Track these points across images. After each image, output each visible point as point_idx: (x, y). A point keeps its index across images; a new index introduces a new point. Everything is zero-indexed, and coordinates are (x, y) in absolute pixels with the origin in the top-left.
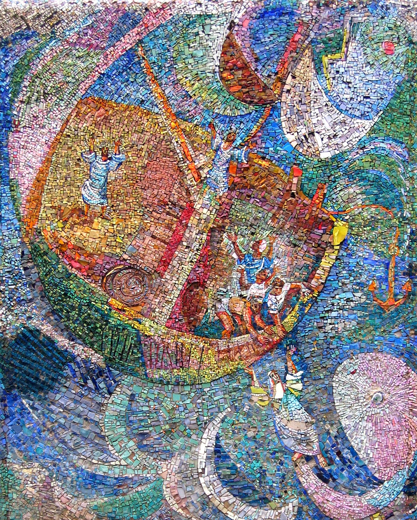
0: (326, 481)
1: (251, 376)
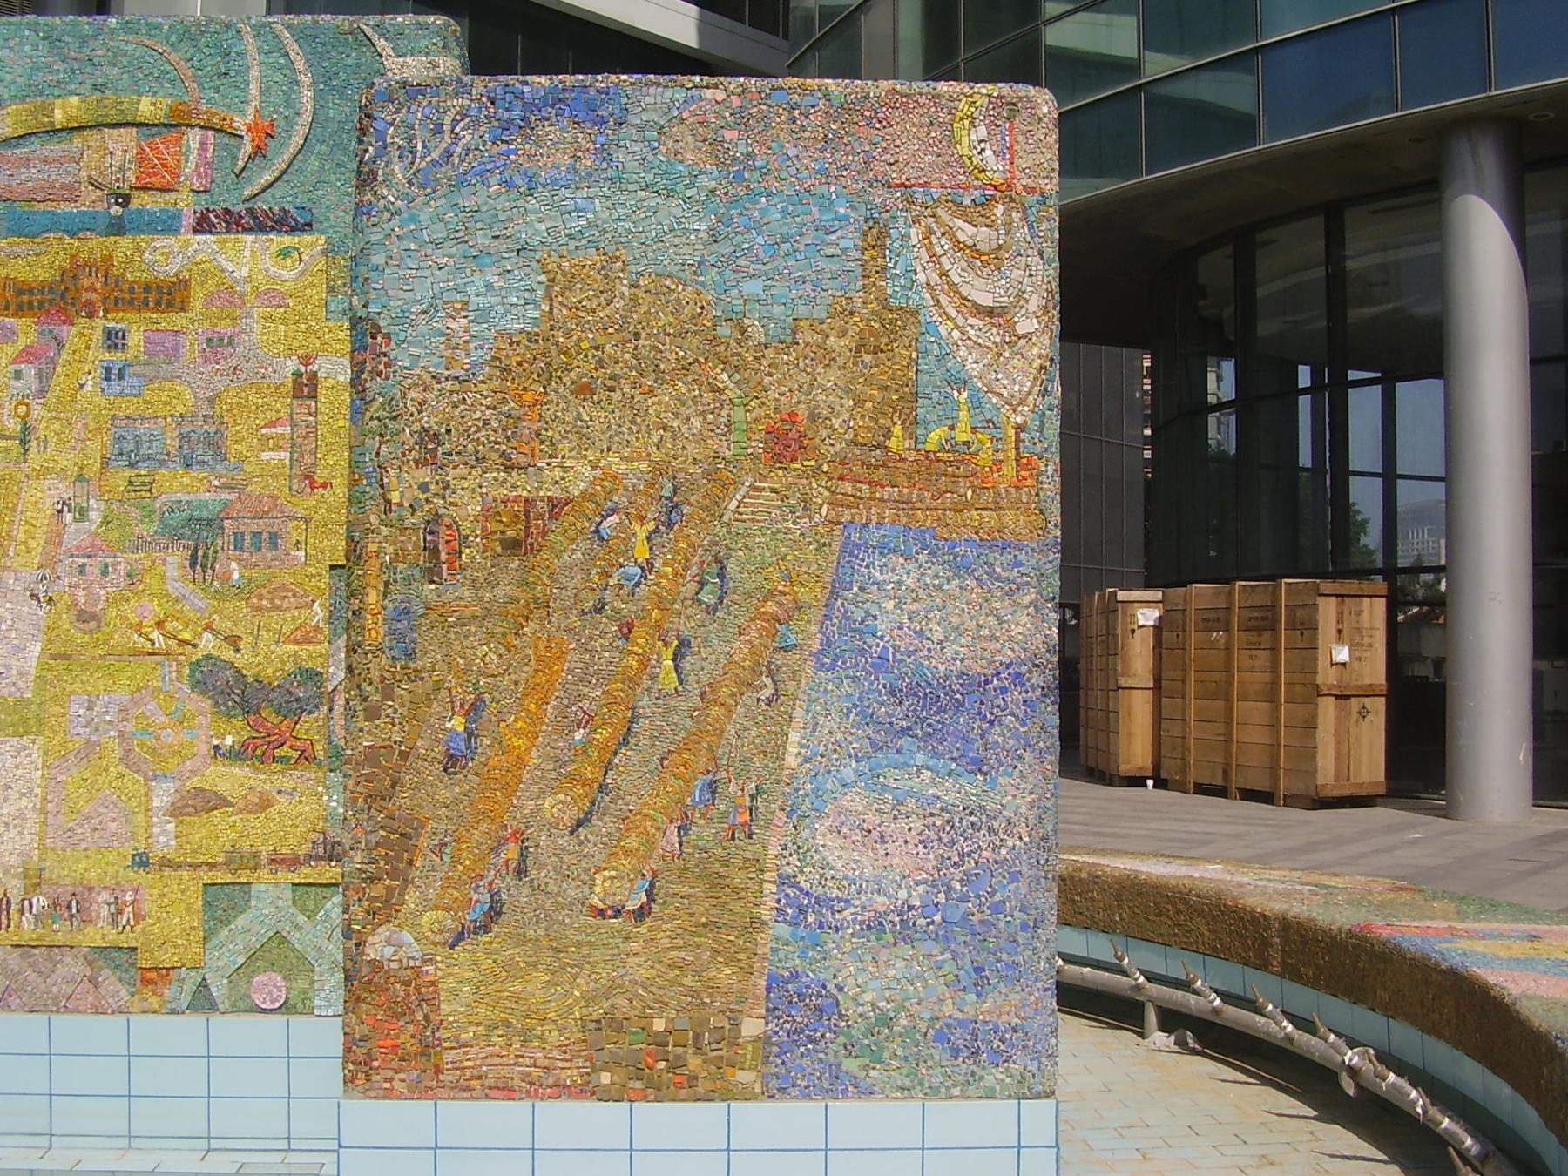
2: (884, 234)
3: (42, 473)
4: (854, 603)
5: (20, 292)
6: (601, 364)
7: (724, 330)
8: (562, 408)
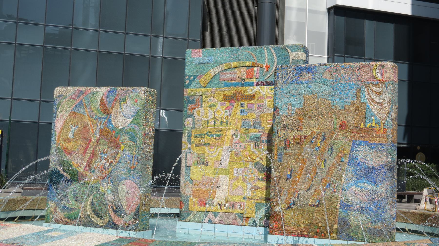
1: (100, 183)
2: (360, 90)
3: (229, 129)
5: (226, 97)
7: (333, 107)
8: (306, 120)
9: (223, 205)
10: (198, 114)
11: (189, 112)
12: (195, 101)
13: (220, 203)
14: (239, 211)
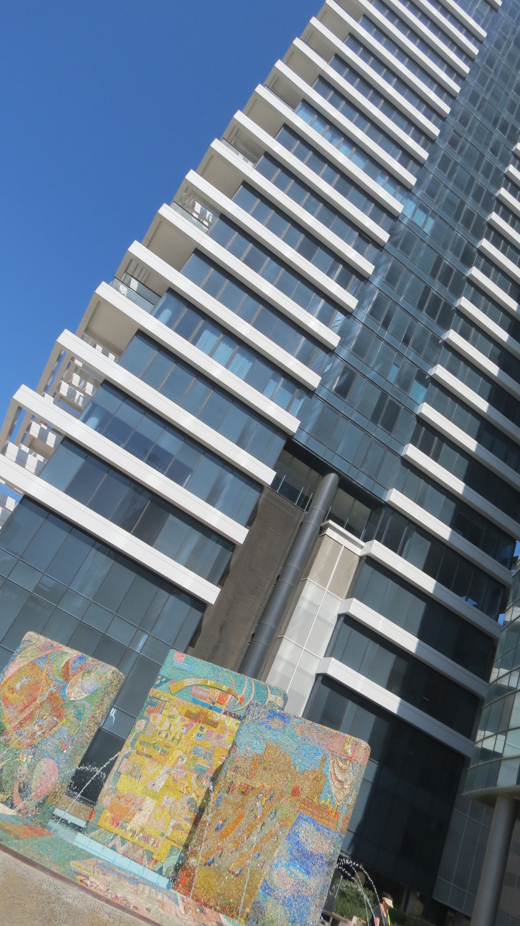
0: (19, 792)
2: (326, 759)
3: (179, 749)
4: (297, 828)
5: (189, 714)
6: (269, 765)
7: (292, 767)
9: (136, 834)
10: (154, 720)
11: (146, 714)
12: (157, 706)
13: (134, 830)
14: (150, 848)
